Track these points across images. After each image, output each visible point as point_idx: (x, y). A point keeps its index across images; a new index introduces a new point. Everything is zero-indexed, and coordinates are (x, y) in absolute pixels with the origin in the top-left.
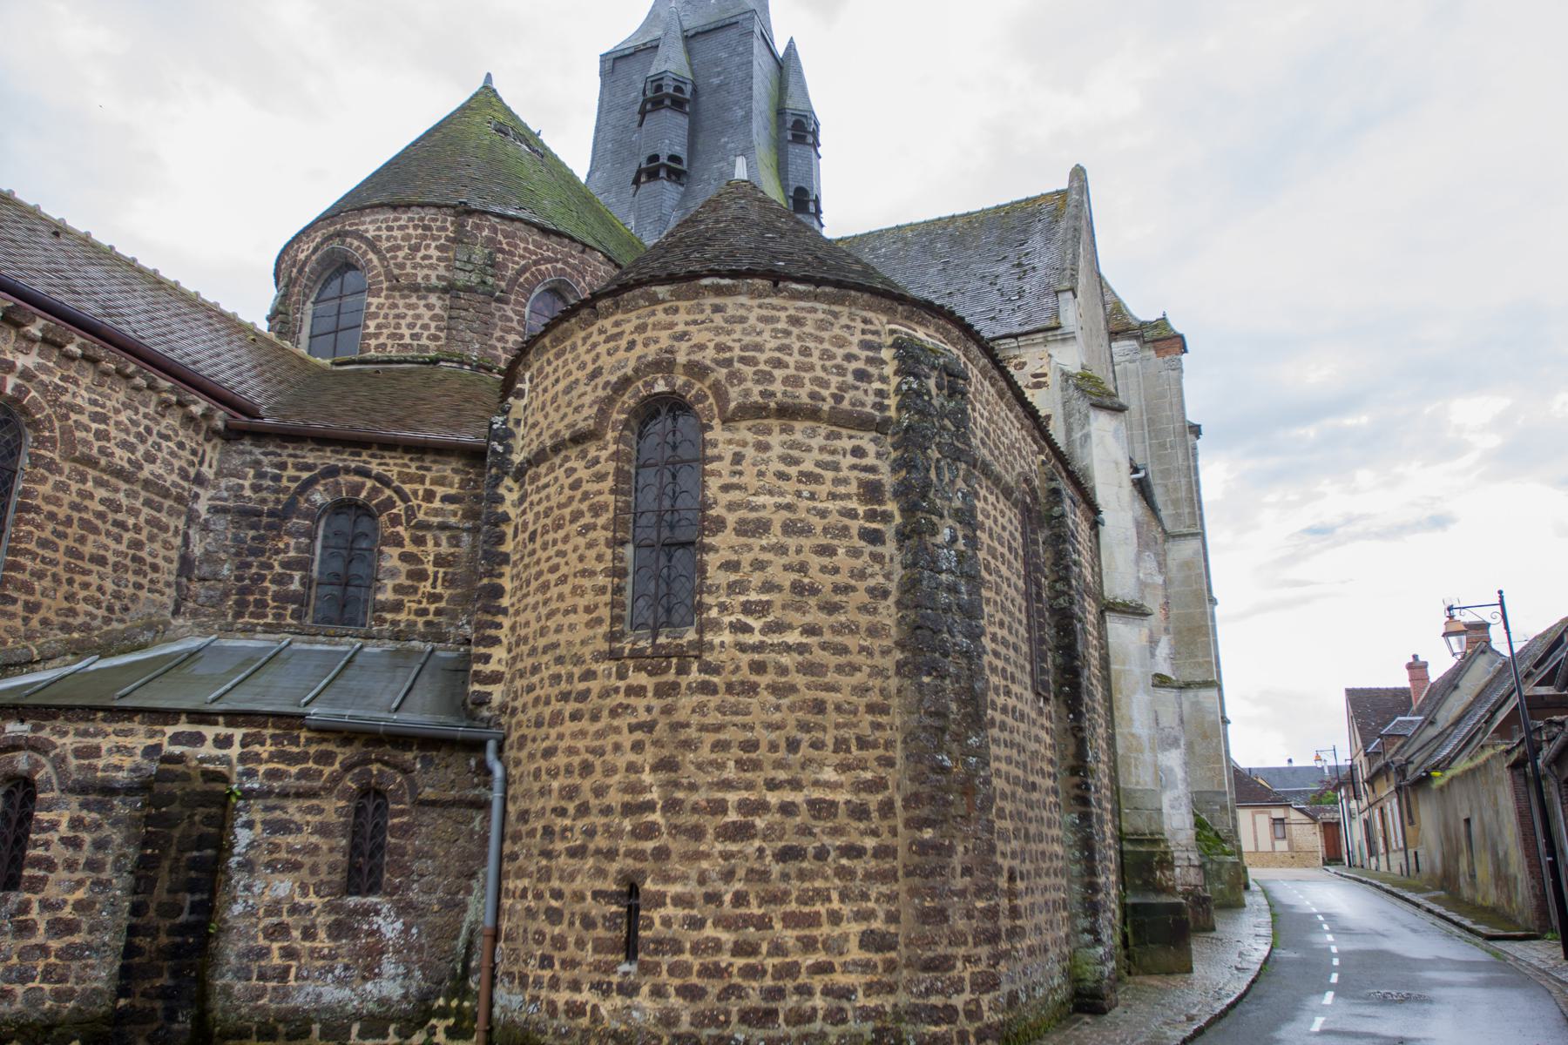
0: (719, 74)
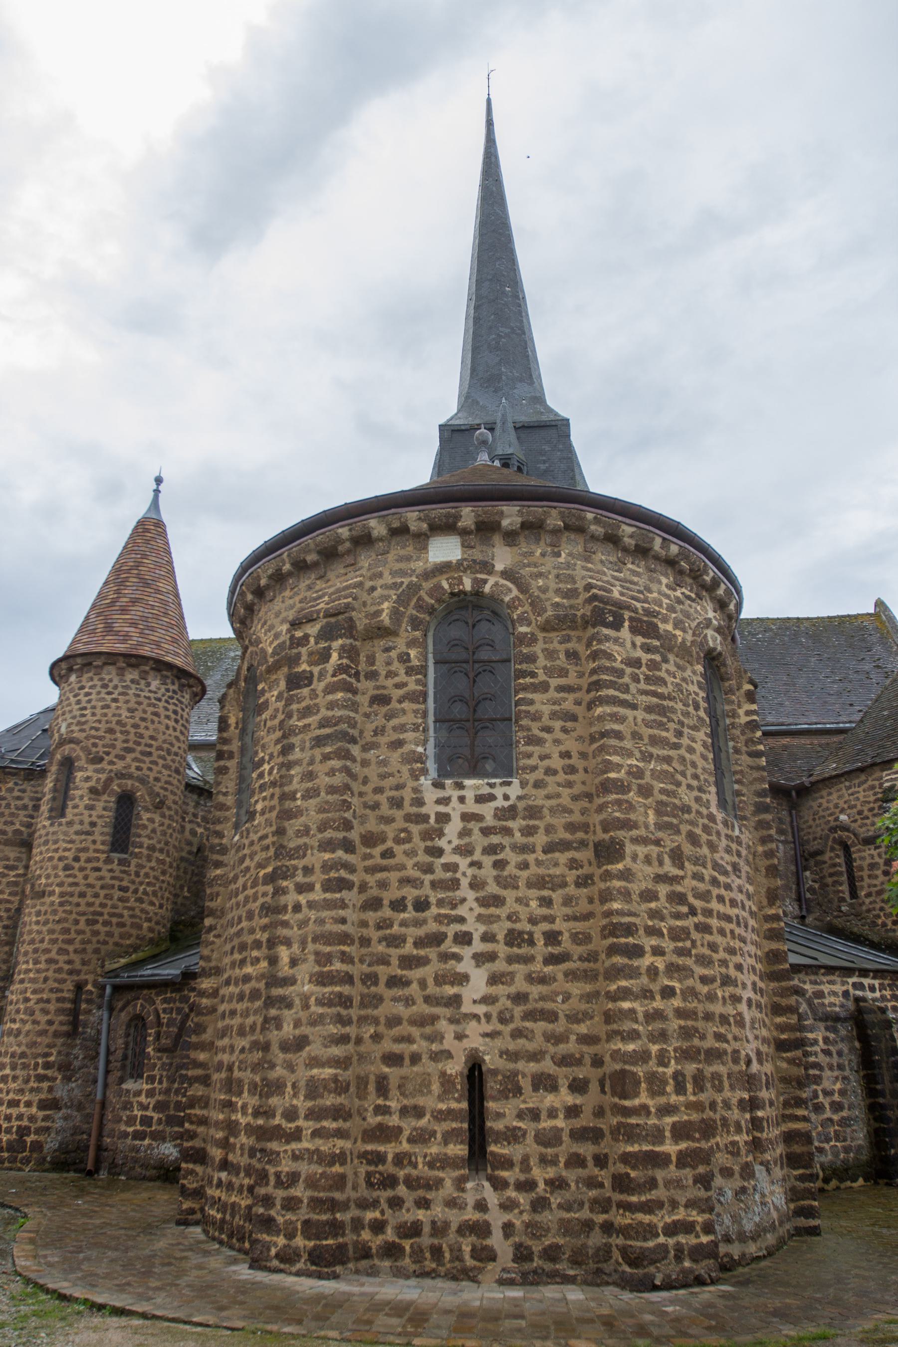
0: (544, 462)
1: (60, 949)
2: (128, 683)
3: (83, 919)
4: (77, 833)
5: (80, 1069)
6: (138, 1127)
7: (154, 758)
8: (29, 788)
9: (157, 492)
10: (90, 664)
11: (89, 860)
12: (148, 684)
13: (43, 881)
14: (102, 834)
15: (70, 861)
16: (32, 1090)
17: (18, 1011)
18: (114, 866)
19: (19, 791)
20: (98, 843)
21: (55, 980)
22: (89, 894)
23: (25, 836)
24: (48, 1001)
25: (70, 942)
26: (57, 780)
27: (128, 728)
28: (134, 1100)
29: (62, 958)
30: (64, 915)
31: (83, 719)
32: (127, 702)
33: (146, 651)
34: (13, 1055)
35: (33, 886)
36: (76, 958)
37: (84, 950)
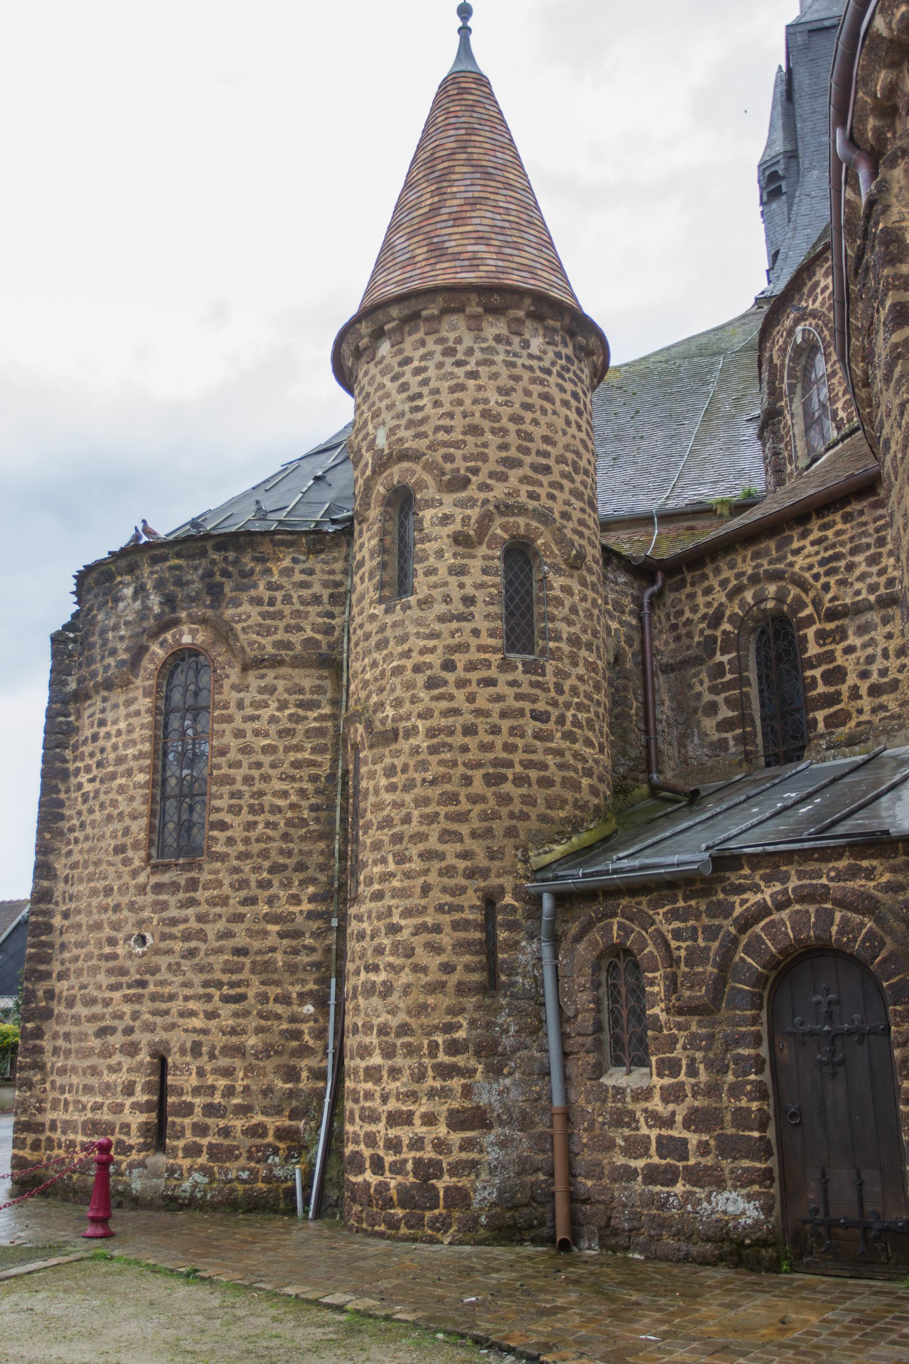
1: (445, 832)
2: (491, 343)
3: (477, 775)
4: (441, 619)
5: (513, 1052)
6: (656, 1160)
7: (555, 477)
8: (318, 567)
9: (465, 32)
10: (414, 317)
11: (471, 666)
12: (526, 345)
13: (390, 712)
14: (487, 616)
15: (437, 671)
16: (432, 1093)
17: (379, 951)
18: (518, 674)
19: (302, 572)
20: (484, 634)
21: (445, 890)
22: (481, 729)
23: (324, 648)
24: (437, 929)
25: (462, 817)
26: (384, 532)
27: (504, 422)
29: (451, 849)
30: (442, 770)
31: (419, 416)
32: (494, 376)
33: (515, 279)
34: (383, 1030)
35: (369, 725)
36: (477, 847)
37: (489, 833)
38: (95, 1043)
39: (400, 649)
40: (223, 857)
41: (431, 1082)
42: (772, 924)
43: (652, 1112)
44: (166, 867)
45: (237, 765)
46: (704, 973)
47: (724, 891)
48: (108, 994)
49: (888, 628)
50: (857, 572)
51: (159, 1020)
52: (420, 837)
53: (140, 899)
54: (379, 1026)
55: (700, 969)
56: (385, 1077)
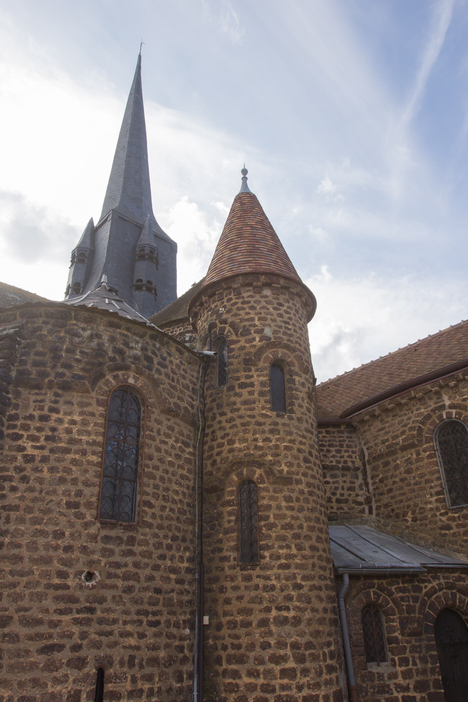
10: (286, 288)
24: (320, 588)
28: (391, 683)
34: (295, 646)
38: (41, 659)
39: (289, 438)
40: (150, 526)
41: (325, 676)
42: (438, 597)
43: (399, 684)
44: (113, 526)
45: (156, 468)
46: (415, 617)
47: (418, 582)
48: (56, 617)
49: (344, 479)
50: (332, 454)
51: (103, 639)
52: (308, 537)
53: (92, 546)
54: (291, 643)
55: (413, 615)
56: (299, 675)
